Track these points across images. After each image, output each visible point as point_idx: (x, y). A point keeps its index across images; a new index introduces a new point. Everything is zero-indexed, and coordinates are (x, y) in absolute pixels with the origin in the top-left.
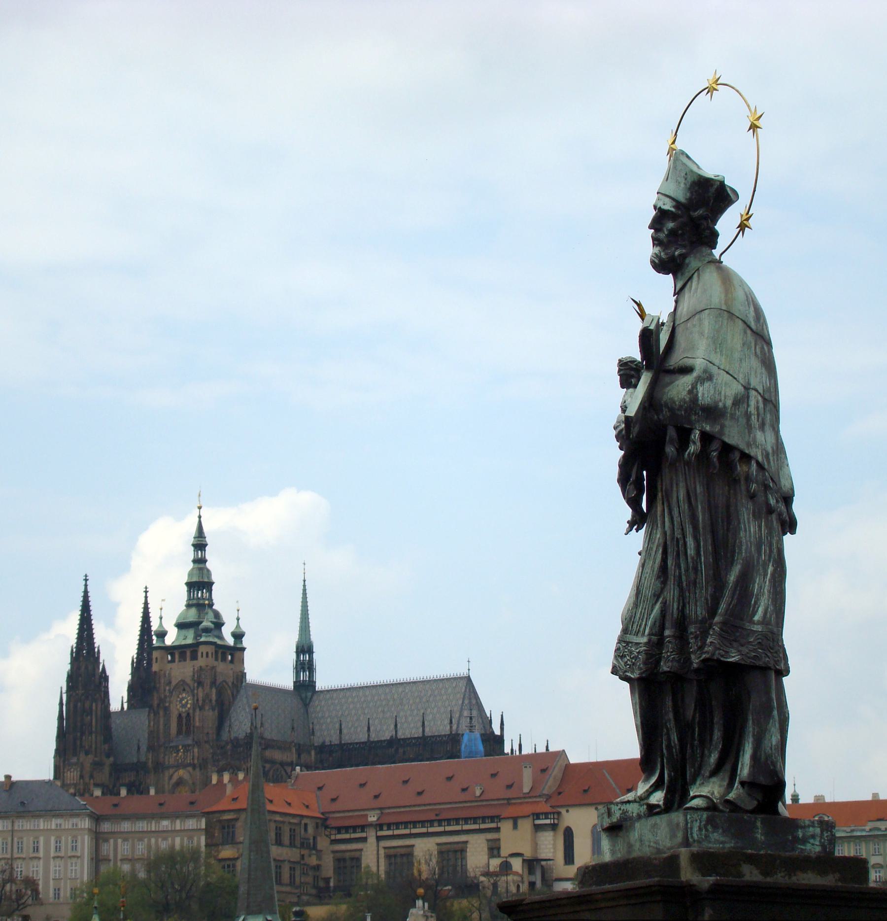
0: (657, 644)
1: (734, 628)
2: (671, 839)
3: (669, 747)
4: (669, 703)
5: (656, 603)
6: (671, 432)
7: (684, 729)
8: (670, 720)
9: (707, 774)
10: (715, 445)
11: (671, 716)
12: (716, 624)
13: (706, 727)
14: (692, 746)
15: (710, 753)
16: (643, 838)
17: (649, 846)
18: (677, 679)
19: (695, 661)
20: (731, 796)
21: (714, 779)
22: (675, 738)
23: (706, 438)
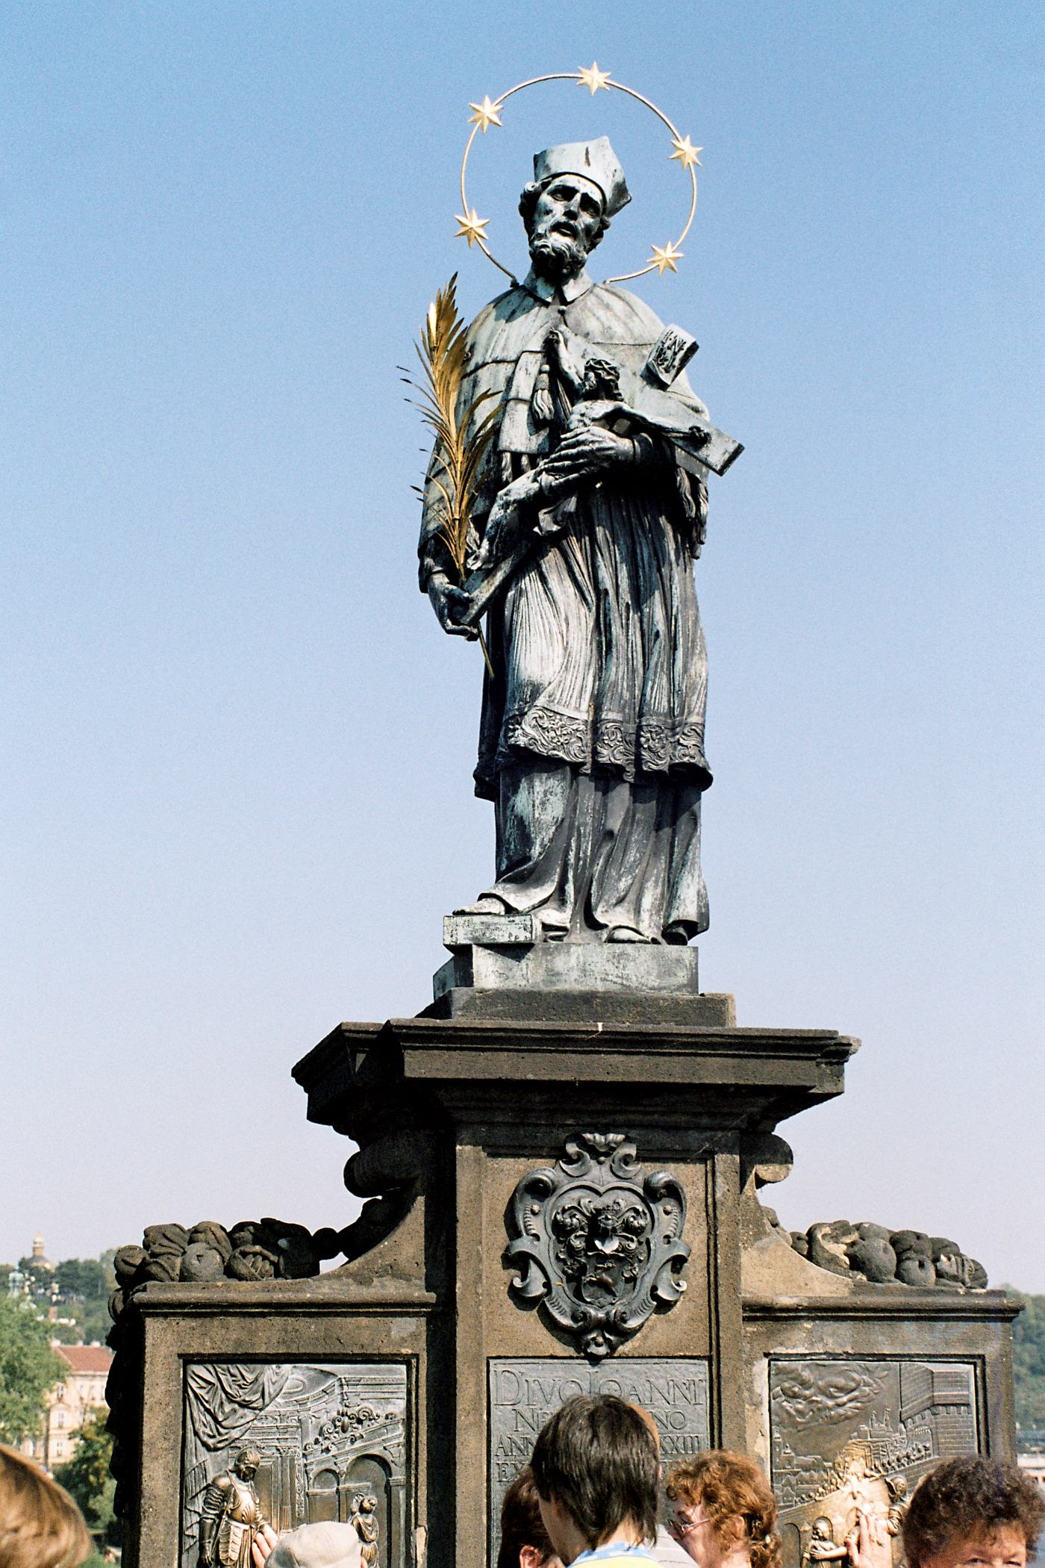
0: (596, 726)
2: (659, 976)
3: (578, 859)
8: (585, 825)
9: (614, 901)
11: (589, 820)
16: (588, 968)
17: (603, 980)
18: (606, 776)
21: (618, 909)
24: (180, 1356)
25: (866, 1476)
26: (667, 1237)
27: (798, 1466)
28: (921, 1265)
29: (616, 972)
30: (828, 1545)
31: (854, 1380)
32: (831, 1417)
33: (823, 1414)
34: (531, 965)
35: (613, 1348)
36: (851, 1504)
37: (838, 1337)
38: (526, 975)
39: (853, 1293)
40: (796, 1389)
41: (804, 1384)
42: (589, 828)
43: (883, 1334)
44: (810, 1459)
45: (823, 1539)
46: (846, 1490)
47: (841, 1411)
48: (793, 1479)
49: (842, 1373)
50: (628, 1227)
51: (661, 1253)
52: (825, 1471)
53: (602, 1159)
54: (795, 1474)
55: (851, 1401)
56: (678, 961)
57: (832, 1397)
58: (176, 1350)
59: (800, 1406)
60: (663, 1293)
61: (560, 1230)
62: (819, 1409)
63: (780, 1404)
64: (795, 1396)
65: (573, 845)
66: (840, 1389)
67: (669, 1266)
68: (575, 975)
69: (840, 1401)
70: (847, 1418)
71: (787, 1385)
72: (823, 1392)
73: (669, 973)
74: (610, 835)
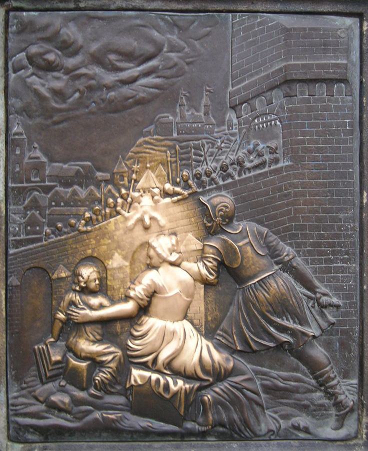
25: (166, 194)
30: (95, 301)
31: (152, 41)
32: (111, 101)
33: (97, 95)
36: (139, 235)
40: (51, 57)
41: (68, 48)
44: (70, 168)
45: (86, 291)
46: (133, 216)
47: (126, 90)
48: (44, 199)
52: (98, 186)
59: (58, 85)
62: (90, 88)
63: (23, 80)
64: (50, 67)
66: (129, 56)
71: (34, 49)
72: (97, 59)
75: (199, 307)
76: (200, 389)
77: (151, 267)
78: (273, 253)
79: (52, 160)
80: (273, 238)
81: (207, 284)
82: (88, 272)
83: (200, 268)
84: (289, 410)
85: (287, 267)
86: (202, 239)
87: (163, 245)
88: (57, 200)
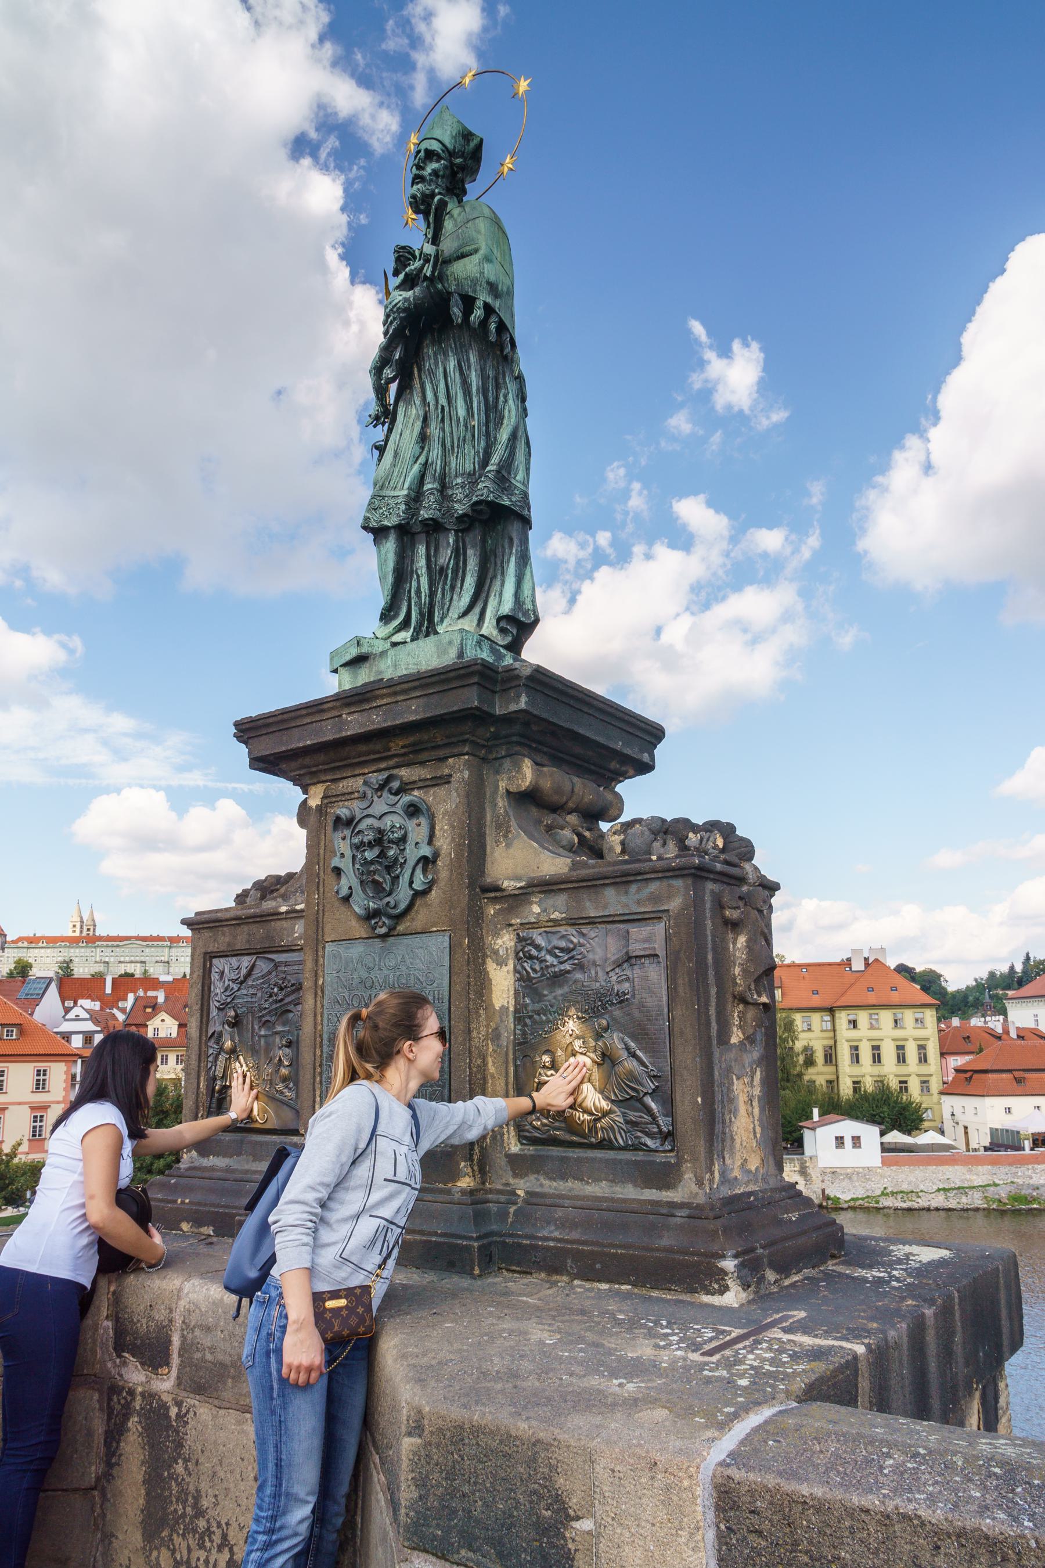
0: (416, 497)
1: (503, 478)
2: (438, 656)
4: (422, 550)
5: (415, 462)
6: (455, 299)
7: (436, 574)
10: (494, 319)
12: (489, 472)
13: (459, 572)
14: (443, 589)
15: (460, 596)
18: (434, 528)
19: (460, 509)
20: (484, 631)
21: (461, 621)
22: (424, 581)
23: (488, 309)
24: (205, 954)
25: (578, 1018)
26: (417, 843)
27: (533, 1011)
28: (664, 844)
29: (414, 661)
30: (549, 1073)
31: (572, 942)
34: (367, 671)
35: (392, 929)
37: (557, 907)
38: (364, 676)
39: (571, 870)
41: (538, 948)
42: (424, 570)
43: (590, 900)
49: (563, 937)
50: (391, 841)
51: (412, 854)
53: (379, 794)
54: (530, 1017)
55: (569, 959)
56: (450, 643)
57: (557, 957)
58: (203, 950)
60: (418, 886)
61: (359, 847)
62: (547, 967)
64: (531, 957)
65: (414, 584)
66: (562, 950)
67: (420, 865)
68: (390, 671)
69: (562, 960)
70: (568, 972)
72: (550, 952)
73: (445, 652)
74: (442, 569)
75: (596, 1076)
76: (595, 1120)
77: (574, 1055)
78: (627, 1048)
79: (533, 1003)
80: (626, 1039)
81: (598, 1064)
82: (546, 1059)
83: (592, 1055)
84: (639, 1134)
85: (634, 1055)
86: (596, 1040)
87: (577, 1044)
88: (534, 1022)
